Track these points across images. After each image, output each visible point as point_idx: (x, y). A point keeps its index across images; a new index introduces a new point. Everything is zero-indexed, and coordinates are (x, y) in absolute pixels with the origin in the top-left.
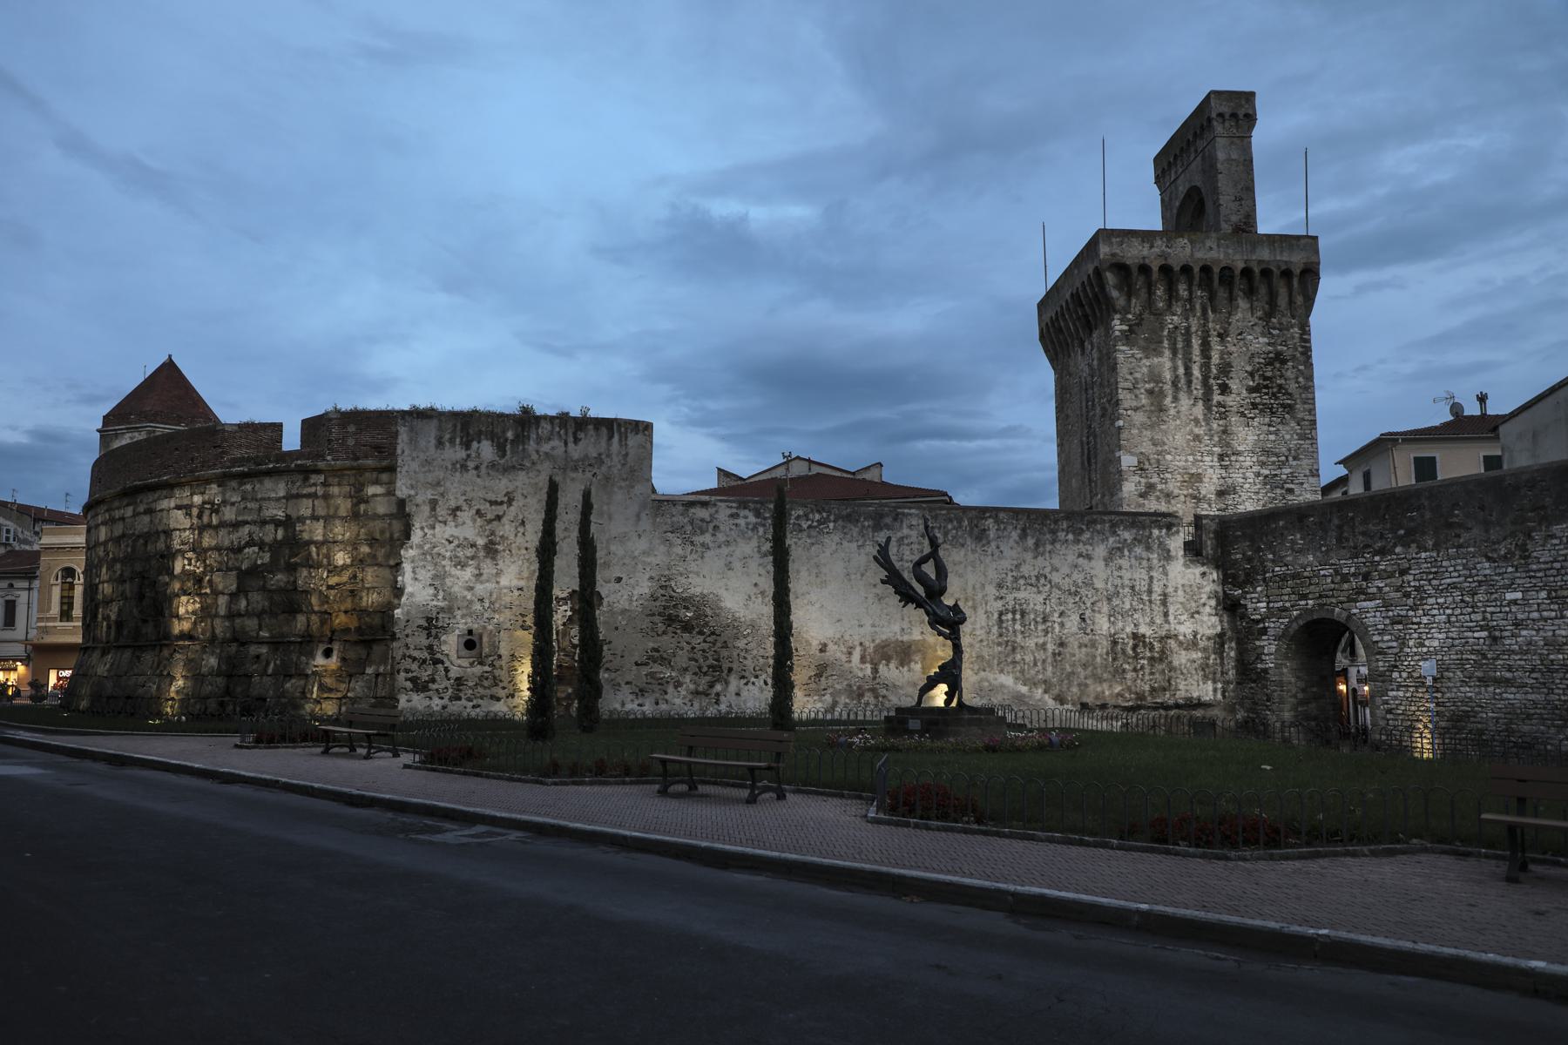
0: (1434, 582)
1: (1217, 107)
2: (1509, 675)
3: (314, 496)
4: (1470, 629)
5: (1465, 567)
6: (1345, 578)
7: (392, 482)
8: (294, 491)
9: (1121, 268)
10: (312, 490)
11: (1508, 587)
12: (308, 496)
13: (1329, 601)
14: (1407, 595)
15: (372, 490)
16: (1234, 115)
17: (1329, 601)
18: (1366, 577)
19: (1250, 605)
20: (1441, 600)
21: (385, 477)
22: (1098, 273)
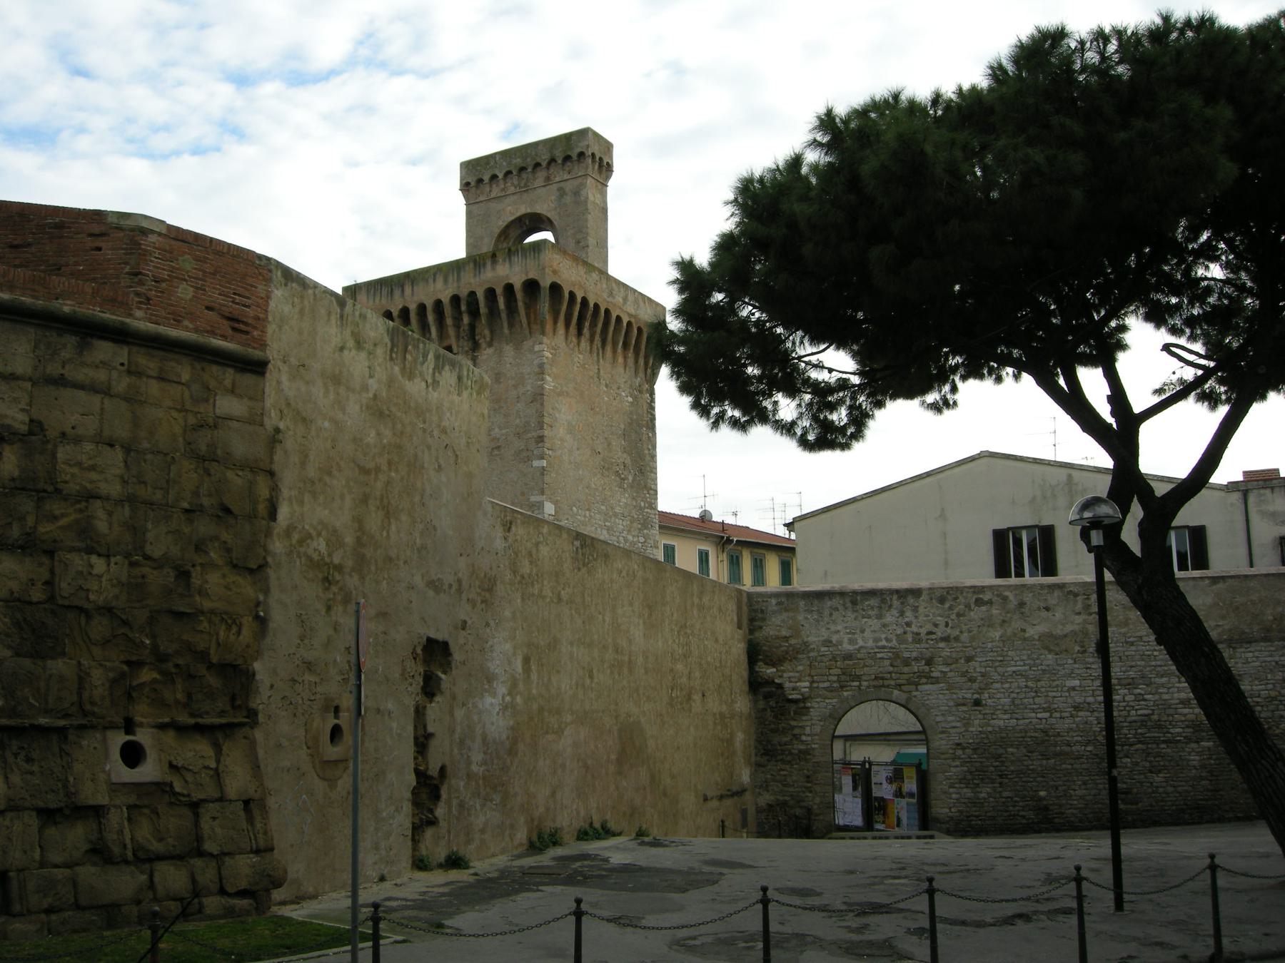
0: (999, 669)
1: (595, 148)
2: (1066, 749)
3: (106, 391)
4: (1033, 710)
5: (1029, 658)
6: (907, 662)
7: (258, 397)
8: (53, 369)
9: (555, 289)
10: (101, 376)
11: (1070, 675)
12: (92, 388)
13: (886, 683)
14: (972, 680)
15: (227, 405)
16: (601, 159)
17: (886, 683)
18: (929, 662)
19: (787, 685)
20: (1007, 686)
21: (247, 380)
22: (532, 286)
